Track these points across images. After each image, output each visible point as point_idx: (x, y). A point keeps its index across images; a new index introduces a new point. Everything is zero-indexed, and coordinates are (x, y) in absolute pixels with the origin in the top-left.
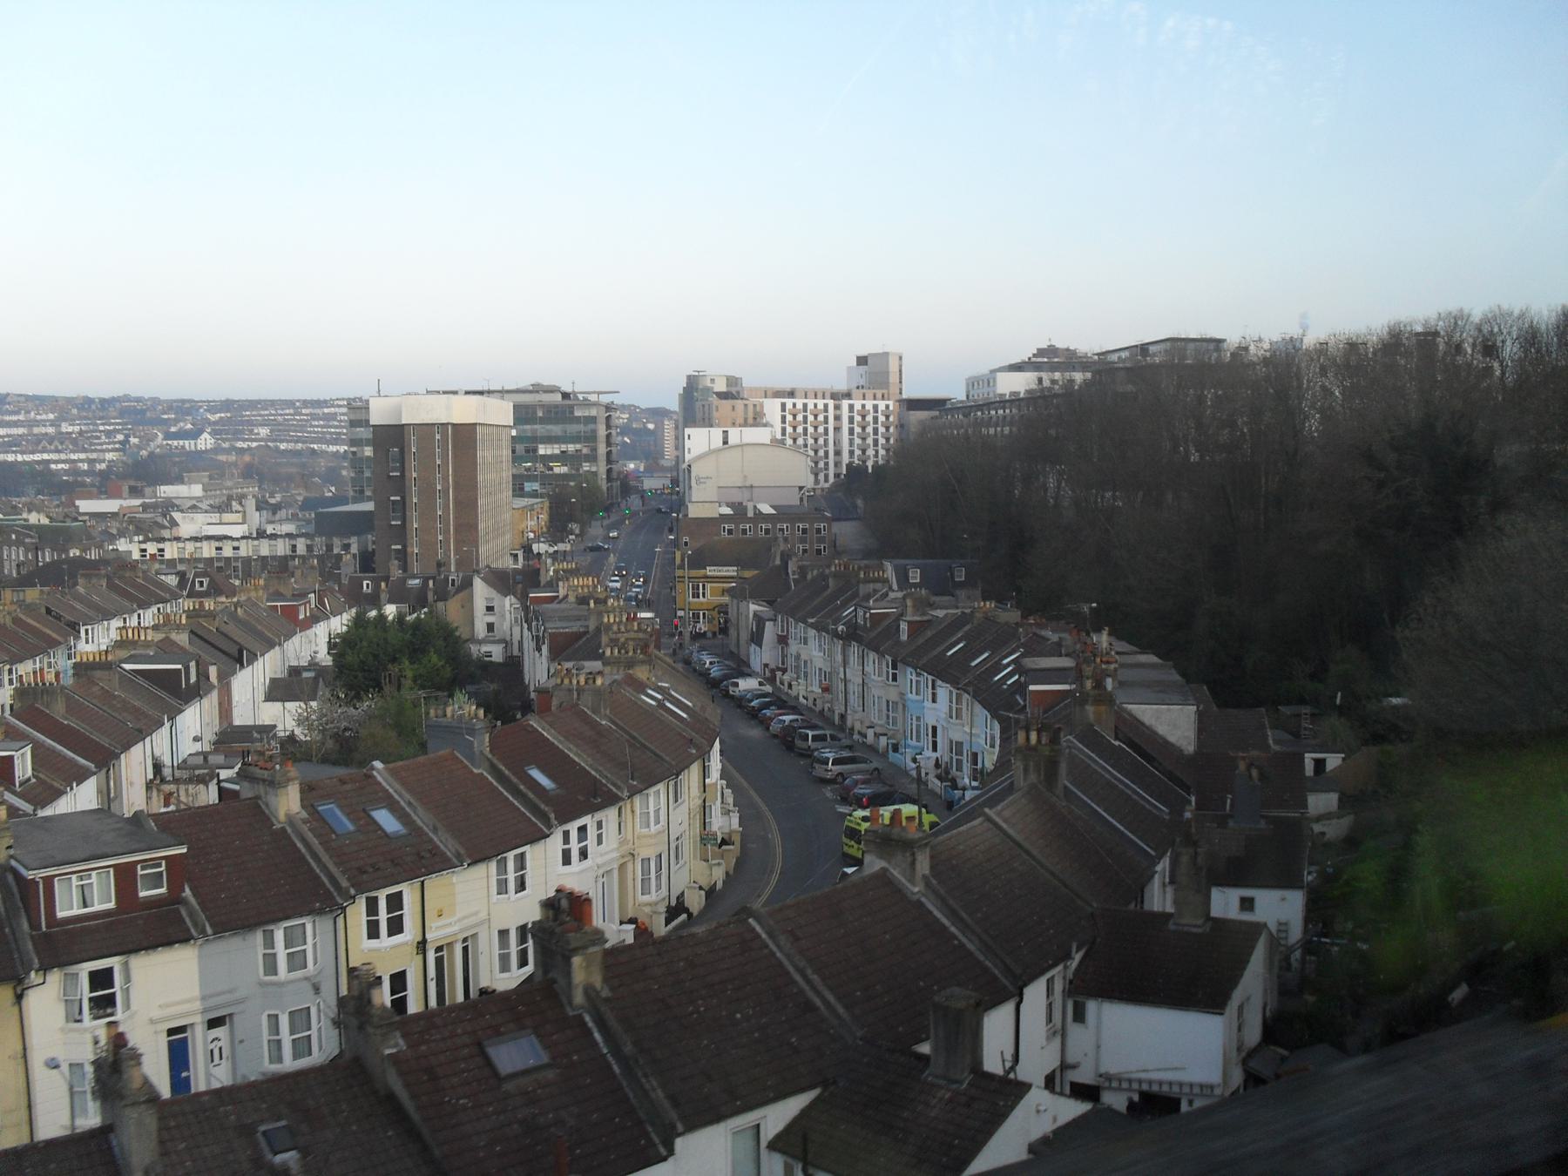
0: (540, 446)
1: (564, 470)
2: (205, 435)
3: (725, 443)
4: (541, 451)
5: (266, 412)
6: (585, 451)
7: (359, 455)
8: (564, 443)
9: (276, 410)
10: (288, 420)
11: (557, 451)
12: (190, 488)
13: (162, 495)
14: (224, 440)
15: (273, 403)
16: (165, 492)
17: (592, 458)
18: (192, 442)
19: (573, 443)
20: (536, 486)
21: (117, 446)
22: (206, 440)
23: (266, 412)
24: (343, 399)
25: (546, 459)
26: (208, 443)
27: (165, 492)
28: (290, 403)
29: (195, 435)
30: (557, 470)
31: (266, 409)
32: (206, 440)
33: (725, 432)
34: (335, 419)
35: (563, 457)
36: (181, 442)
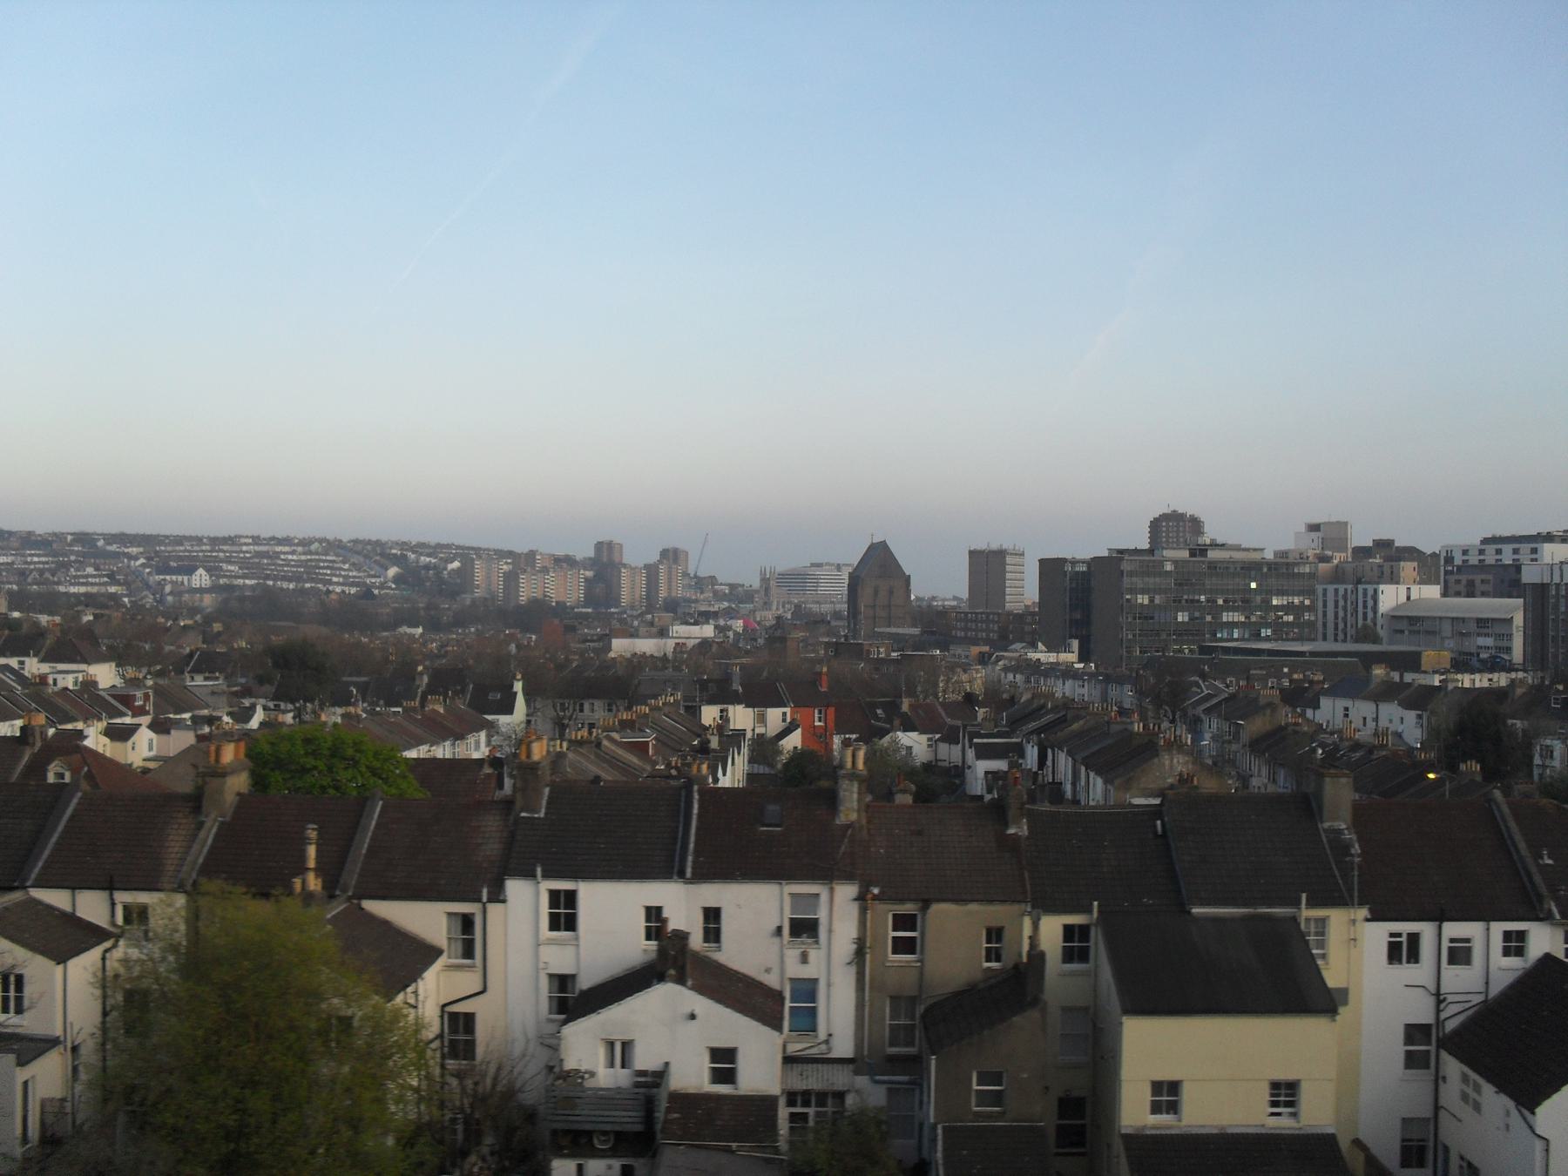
0: (1274, 598)
1: (1291, 618)
2: (201, 571)
3: (1408, 598)
4: (1275, 602)
5: (182, 548)
6: (1307, 602)
7: (1133, 601)
8: (1288, 595)
9: (192, 545)
10: (207, 556)
11: (1285, 603)
12: (701, 628)
13: (674, 635)
14: (218, 577)
15: (179, 540)
16: (677, 632)
17: (1311, 609)
18: (186, 578)
19: (1298, 595)
20: (1269, 632)
21: (106, 579)
22: (201, 575)
23: (182, 548)
24: (247, 537)
25: (1278, 608)
26: (203, 580)
27: (677, 632)
28: (199, 540)
29: (190, 571)
30: (1285, 618)
31: (182, 545)
32: (201, 575)
33: (1409, 589)
34: (279, 558)
35: (1288, 608)
36: (180, 578)
